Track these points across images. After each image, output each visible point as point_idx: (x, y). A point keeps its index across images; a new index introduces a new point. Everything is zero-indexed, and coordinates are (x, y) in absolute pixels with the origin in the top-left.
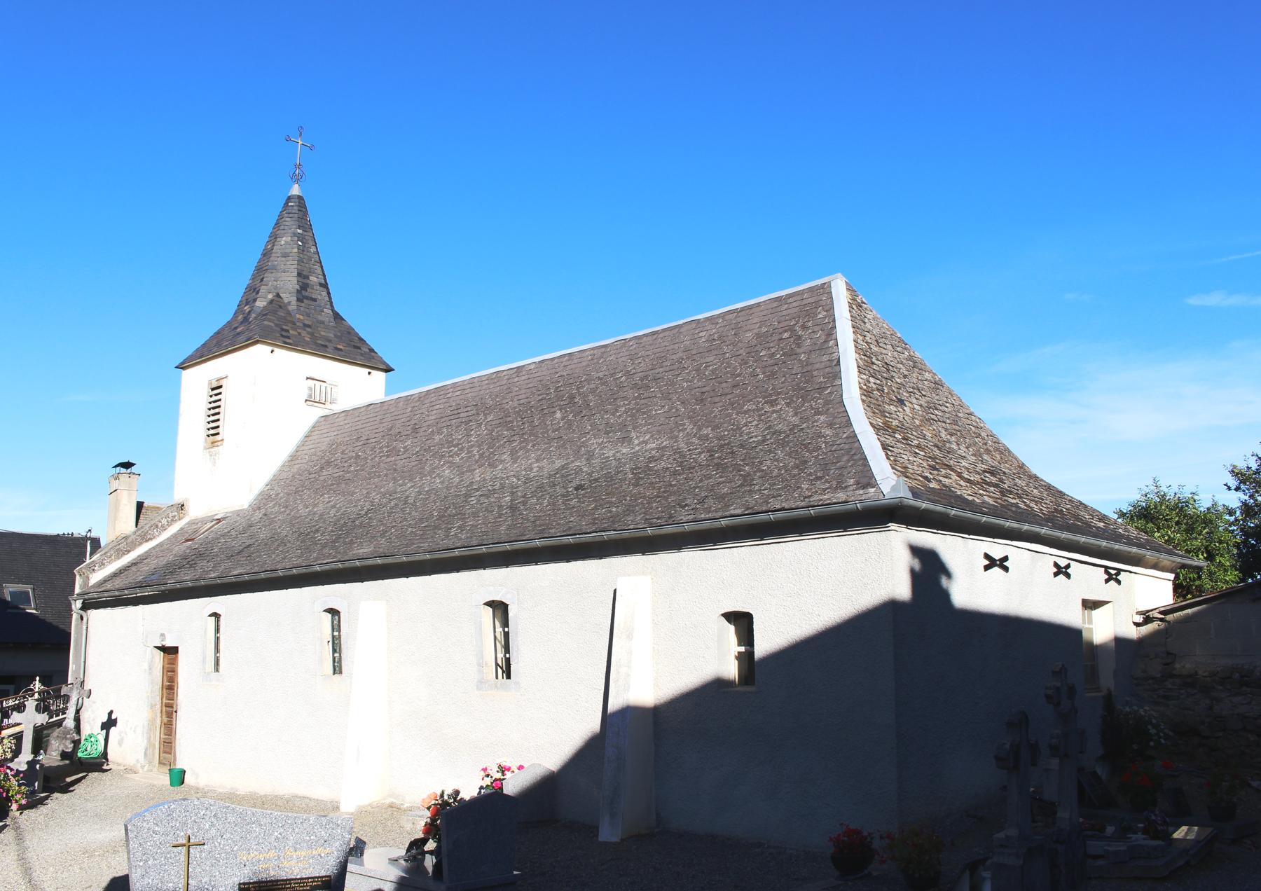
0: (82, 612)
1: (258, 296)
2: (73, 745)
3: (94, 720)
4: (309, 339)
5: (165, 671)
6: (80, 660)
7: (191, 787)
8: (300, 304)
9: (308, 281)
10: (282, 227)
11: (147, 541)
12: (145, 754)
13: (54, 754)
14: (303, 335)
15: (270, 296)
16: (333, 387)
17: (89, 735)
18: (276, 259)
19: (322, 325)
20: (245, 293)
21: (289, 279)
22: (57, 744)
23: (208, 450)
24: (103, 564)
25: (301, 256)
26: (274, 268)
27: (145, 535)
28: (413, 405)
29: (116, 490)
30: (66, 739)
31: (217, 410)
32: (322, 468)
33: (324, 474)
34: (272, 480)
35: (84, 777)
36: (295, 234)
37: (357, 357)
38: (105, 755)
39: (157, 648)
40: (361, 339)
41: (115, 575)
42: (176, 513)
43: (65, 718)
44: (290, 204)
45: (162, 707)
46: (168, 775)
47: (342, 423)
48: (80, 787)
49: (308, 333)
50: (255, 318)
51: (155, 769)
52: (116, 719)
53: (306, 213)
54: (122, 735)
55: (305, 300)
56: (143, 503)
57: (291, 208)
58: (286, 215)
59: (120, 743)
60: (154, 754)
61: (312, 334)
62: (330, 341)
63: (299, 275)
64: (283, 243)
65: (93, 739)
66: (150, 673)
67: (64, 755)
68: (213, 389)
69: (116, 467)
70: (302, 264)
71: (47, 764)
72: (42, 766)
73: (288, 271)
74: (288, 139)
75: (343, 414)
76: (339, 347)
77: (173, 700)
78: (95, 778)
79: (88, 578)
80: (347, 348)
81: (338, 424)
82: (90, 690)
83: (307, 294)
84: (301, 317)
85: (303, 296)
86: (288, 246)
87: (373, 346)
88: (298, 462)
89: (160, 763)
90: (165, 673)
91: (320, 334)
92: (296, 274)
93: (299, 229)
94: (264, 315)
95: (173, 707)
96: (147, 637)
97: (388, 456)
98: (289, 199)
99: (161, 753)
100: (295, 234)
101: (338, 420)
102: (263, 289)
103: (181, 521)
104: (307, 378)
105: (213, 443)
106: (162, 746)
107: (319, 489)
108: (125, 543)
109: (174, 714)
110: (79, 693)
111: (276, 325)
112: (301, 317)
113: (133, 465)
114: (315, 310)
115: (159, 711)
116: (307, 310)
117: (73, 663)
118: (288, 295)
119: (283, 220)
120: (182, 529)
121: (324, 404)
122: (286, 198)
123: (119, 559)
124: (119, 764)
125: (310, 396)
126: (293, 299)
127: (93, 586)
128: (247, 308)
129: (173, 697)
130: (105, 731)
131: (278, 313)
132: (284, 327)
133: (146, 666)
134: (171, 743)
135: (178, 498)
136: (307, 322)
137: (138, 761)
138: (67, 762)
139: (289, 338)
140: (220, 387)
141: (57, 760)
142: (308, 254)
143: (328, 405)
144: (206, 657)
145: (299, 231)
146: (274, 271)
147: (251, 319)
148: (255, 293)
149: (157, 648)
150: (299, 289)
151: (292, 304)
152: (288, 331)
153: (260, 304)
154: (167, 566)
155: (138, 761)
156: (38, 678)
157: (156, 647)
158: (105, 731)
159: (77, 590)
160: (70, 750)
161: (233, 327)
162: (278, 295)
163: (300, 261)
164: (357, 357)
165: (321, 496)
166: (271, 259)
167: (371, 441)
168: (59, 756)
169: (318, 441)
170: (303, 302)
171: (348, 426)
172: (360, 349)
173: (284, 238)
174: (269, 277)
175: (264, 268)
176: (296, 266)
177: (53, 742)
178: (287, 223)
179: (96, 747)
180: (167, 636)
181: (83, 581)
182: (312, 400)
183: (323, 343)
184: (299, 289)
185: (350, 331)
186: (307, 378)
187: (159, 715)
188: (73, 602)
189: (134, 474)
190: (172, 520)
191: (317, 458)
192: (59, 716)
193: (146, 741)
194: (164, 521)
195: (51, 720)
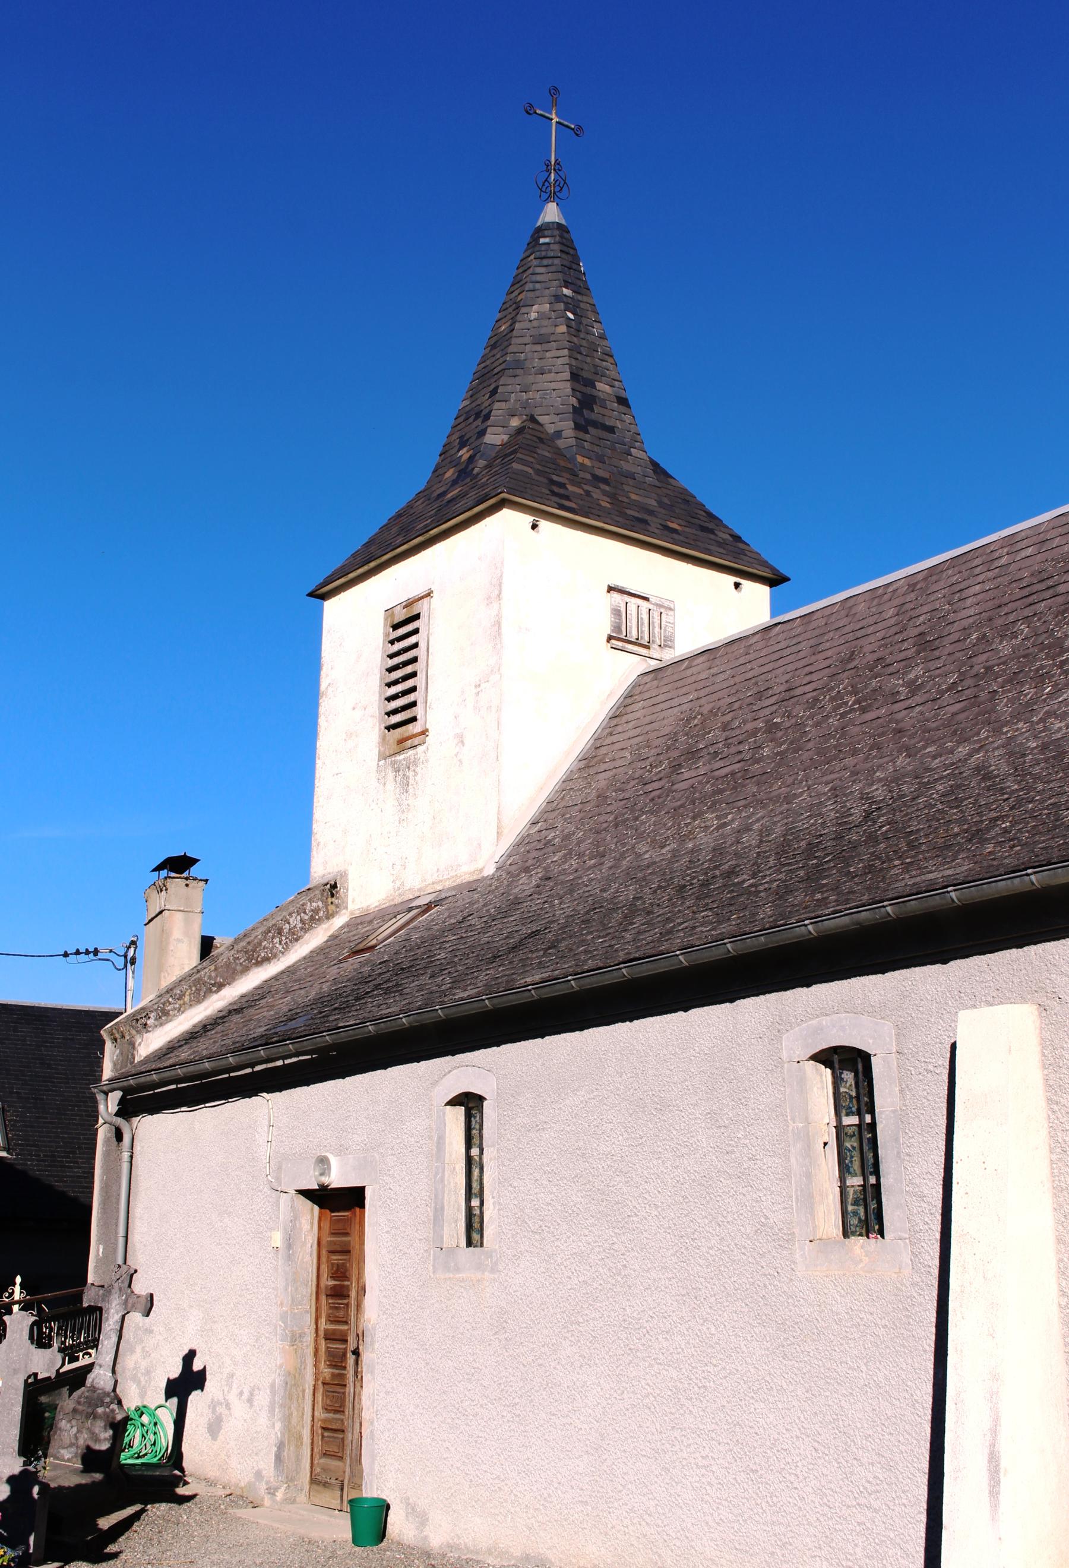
0: (119, 1121)
1: (489, 423)
2: (111, 1432)
3: (148, 1372)
4: (608, 505)
5: (324, 1252)
6: (117, 1233)
7: (408, 1551)
8: (581, 435)
9: (594, 392)
10: (529, 286)
11: (259, 964)
12: (278, 1458)
13: (67, 1454)
14: (595, 496)
15: (515, 422)
16: (662, 610)
17: (137, 1409)
18: (521, 347)
19: (631, 482)
20: (453, 427)
21: (553, 385)
22: (75, 1430)
23: (389, 760)
24: (166, 1013)
25: (575, 340)
26: (519, 365)
27: (253, 951)
28: (897, 602)
29: (161, 912)
30: (94, 1416)
31: (409, 669)
32: (676, 768)
33: (686, 776)
34: (544, 812)
35: (136, 1516)
36: (558, 298)
37: (712, 548)
38: (176, 1456)
39: (306, 1193)
40: (710, 516)
41: (191, 1036)
42: (320, 903)
43: (92, 1365)
44: (542, 241)
45: (316, 1341)
46: (348, 1516)
47: (703, 676)
48: (131, 1543)
49: (605, 493)
50: (488, 466)
51: (302, 1498)
52: (204, 1370)
53: (576, 260)
54: (219, 1409)
55: (590, 429)
56: (213, 939)
57: (543, 248)
58: (536, 262)
59: (214, 1428)
60: (298, 1460)
61: (613, 497)
62: (651, 513)
63: (575, 377)
64: (533, 315)
65: (145, 1419)
66: (289, 1258)
67: (91, 1459)
68: (395, 627)
69: (158, 868)
70: (579, 356)
71: (53, 1479)
72: (44, 1487)
73: (550, 372)
74: (530, 110)
75: (701, 659)
76: (671, 525)
77: (346, 1323)
78: (163, 1518)
79: (132, 1045)
80: (687, 529)
81: (693, 679)
82: (152, 1295)
83: (593, 416)
84: (587, 462)
85: (586, 420)
86: (545, 322)
87: (738, 531)
88: (603, 767)
89: (314, 1481)
90: (324, 1259)
91: (628, 498)
92: (567, 375)
93: (567, 288)
94: (506, 456)
95: (346, 1341)
96: (280, 1168)
97: (863, 710)
98: (540, 231)
99: (317, 1457)
100: (558, 298)
101: (689, 672)
102: (499, 410)
103: (331, 921)
104: (610, 589)
105: (401, 742)
106: (318, 1440)
107: (681, 806)
108: (212, 967)
109: (351, 1359)
110: (126, 1300)
111: (538, 472)
112: (587, 462)
113: (193, 861)
114: (613, 449)
115: (310, 1351)
116: (596, 449)
117: (99, 1242)
118: (556, 419)
119: (530, 271)
120: (333, 937)
121: (648, 647)
122: (531, 232)
123: (199, 1002)
124: (211, 1483)
125: (617, 628)
126: (567, 427)
127: (147, 1060)
128: (464, 453)
129: (347, 1315)
130: (174, 1401)
131: (539, 451)
132: (555, 478)
133: (277, 1239)
134: (343, 1431)
135: (320, 869)
136: (600, 473)
137: (258, 1474)
138: (98, 1476)
139: (567, 498)
140: (417, 617)
141: (74, 1471)
142: (589, 337)
143: (655, 652)
144: (443, 1208)
145: (566, 291)
146: (519, 372)
147: (476, 470)
148: (479, 421)
149: (306, 1193)
150: (576, 404)
151: (564, 434)
152: (562, 486)
153: (495, 437)
154: (319, 1001)
155: (258, 1474)
156: (18, 1279)
157: (302, 1192)
158: (174, 1401)
159: (107, 1072)
160: (105, 1446)
161: (435, 494)
162: (532, 419)
163: (574, 350)
164: (712, 548)
165: (694, 818)
166: (511, 349)
167: (798, 692)
168: (80, 1461)
169: (648, 719)
170: (587, 432)
171: (722, 677)
172: (713, 533)
173: (534, 307)
174: (509, 386)
175: (496, 371)
176: (566, 360)
177: (63, 1424)
178: (539, 278)
179: (152, 1437)
180: (334, 1161)
181: (122, 1053)
182: (623, 636)
183: (636, 514)
184: (576, 404)
185: (688, 498)
186: (610, 589)
187: (310, 1360)
188: (100, 1097)
189: (195, 879)
190: (312, 918)
191: (654, 752)
192: (77, 1359)
193: (278, 1425)
194: (295, 921)
195: (68, 1367)
